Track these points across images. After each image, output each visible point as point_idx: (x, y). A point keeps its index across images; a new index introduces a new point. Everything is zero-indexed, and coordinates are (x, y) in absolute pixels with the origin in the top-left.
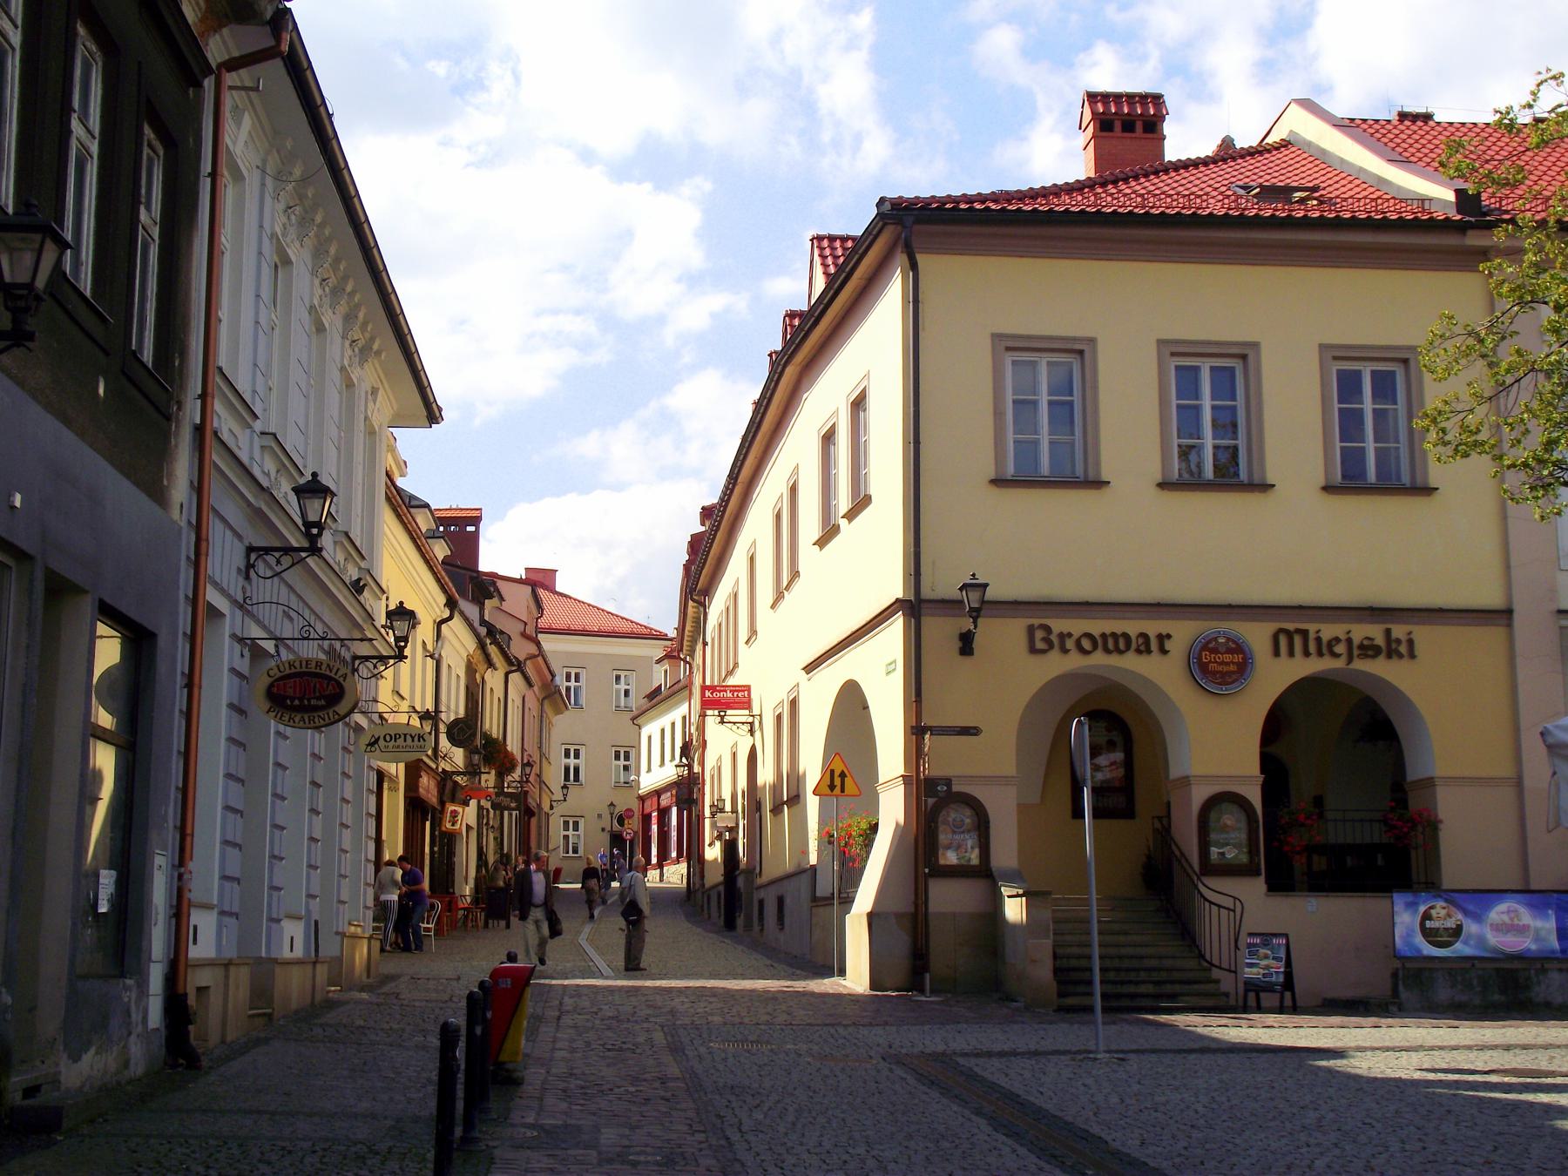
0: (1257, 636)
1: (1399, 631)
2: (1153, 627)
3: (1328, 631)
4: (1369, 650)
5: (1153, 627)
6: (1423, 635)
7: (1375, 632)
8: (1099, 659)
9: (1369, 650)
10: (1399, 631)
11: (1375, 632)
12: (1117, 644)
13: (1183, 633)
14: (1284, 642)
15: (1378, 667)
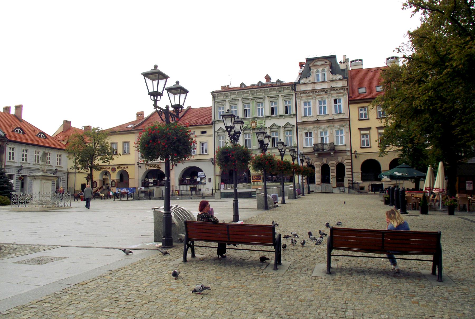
0: (116, 167)
1: (127, 166)
2: (109, 167)
3: (122, 166)
4: (124, 168)
5: (109, 167)
6: (129, 166)
7: (125, 166)
8: (105, 170)
9: (124, 168)
10: (127, 166)
11: (125, 166)
12: (106, 168)
13: (111, 167)
14: (118, 167)
15: (125, 169)
